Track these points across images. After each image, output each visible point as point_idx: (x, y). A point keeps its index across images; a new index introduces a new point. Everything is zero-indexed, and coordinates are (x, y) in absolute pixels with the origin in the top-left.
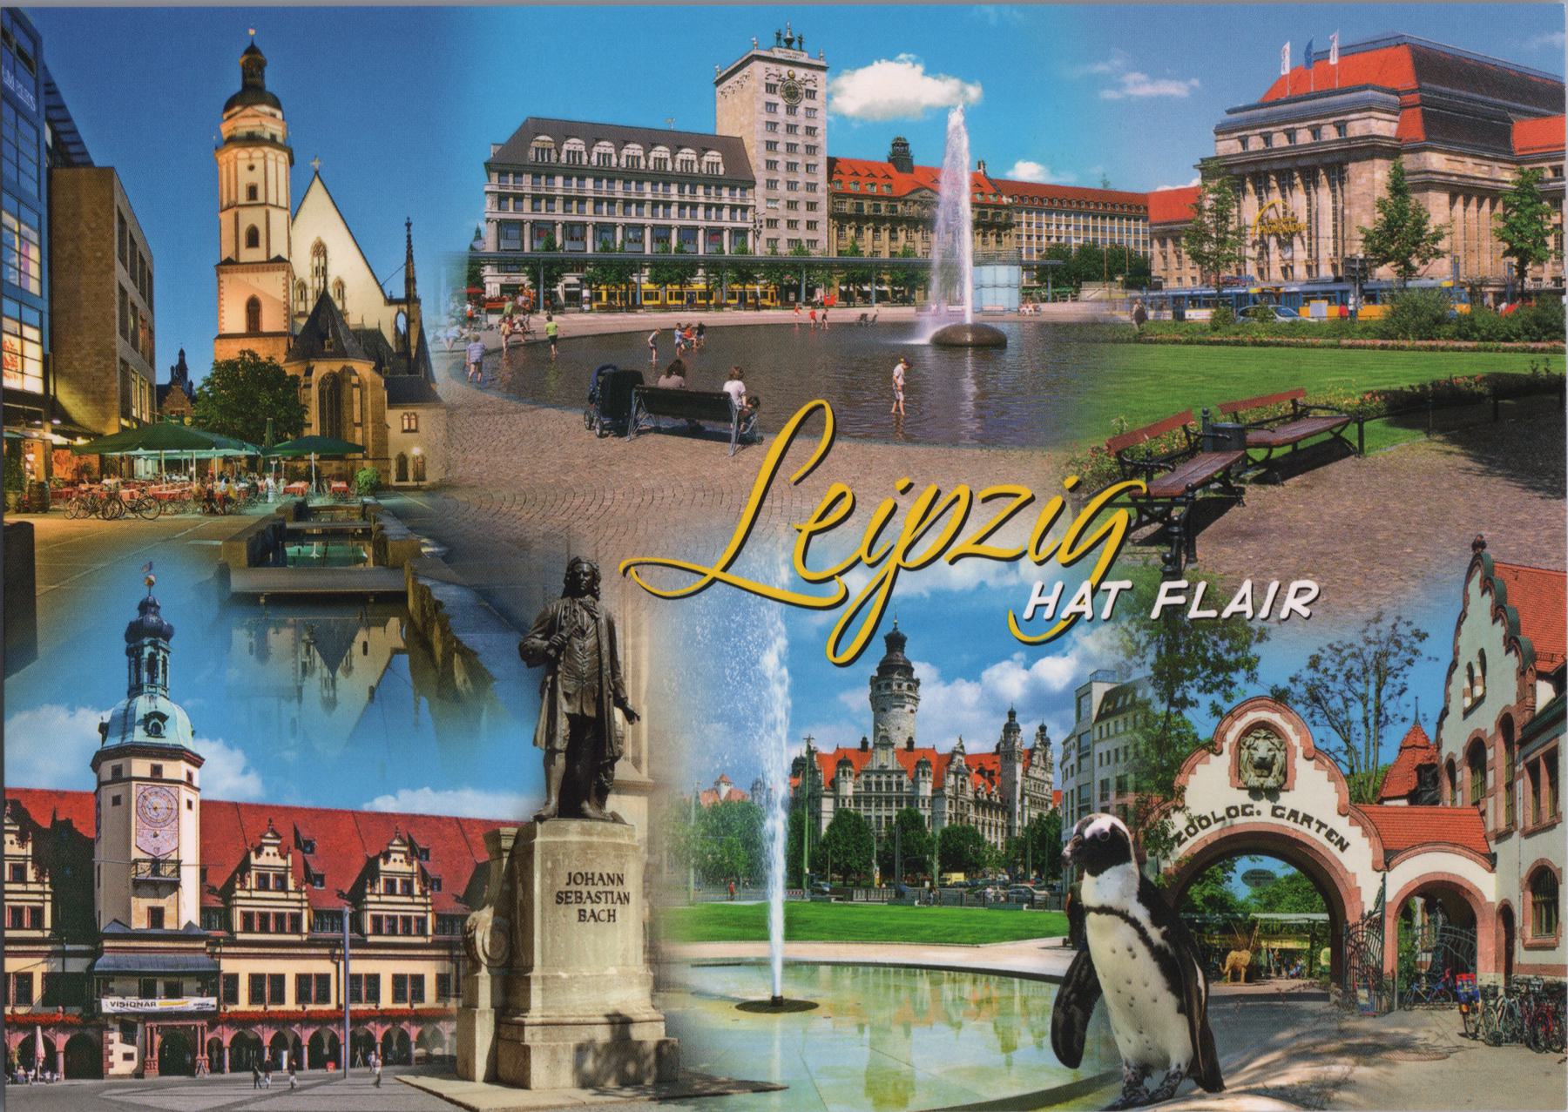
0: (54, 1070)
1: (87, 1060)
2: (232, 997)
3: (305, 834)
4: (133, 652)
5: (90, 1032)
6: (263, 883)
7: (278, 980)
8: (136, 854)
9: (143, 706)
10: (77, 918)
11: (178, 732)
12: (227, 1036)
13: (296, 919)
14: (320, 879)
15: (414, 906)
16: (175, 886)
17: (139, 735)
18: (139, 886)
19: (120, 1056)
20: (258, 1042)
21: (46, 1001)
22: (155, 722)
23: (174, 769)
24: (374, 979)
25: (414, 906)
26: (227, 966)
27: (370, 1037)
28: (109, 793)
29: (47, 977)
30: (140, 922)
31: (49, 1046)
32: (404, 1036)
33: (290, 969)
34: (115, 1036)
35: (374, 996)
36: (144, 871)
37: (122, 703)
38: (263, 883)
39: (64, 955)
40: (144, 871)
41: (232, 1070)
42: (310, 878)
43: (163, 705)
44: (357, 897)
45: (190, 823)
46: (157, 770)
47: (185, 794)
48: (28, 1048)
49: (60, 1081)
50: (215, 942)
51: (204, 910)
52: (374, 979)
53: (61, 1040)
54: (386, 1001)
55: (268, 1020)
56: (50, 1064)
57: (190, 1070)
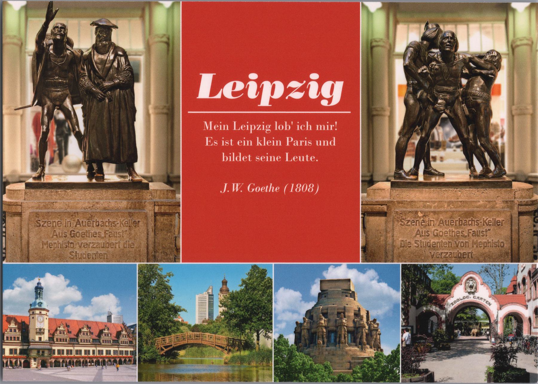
0: (20, 365)
1: (27, 365)
2: (54, 353)
3: (68, 324)
4: (36, 292)
5: (28, 360)
6: (60, 333)
7: (63, 350)
8: (36, 327)
9: (38, 301)
10: (25, 338)
11: (44, 306)
12: (53, 360)
13: (66, 339)
14: (71, 332)
15: (89, 337)
16: (43, 333)
17: (37, 306)
18: (37, 333)
19: (33, 364)
20: (59, 362)
21: (20, 353)
22: (40, 304)
23: (43, 312)
24: (81, 351)
25: (89, 337)
26: (53, 348)
27: (80, 361)
28: (31, 317)
29: (20, 349)
30: (37, 339)
31: (20, 362)
32: (86, 361)
33: (65, 349)
34: (33, 360)
35: (81, 354)
36: (38, 330)
37: (34, 300)
38: (60, 333)
39: (23, 345)
40: (38, 330)
41: (55, 367)
42: (69, 332)
43: (42, 301)
44: (77, 335)
45: (46, 322)
46: (40, 312)
47: (45, 317)
48: (16, 362)
49: (23, 369)
50: (52, 343)
51: (49, 338)
52: (81, 351)
53: (22, 361)
54: (83, 354)
55: (62, 358)
56: (20, 365)
57: (46, 367)
